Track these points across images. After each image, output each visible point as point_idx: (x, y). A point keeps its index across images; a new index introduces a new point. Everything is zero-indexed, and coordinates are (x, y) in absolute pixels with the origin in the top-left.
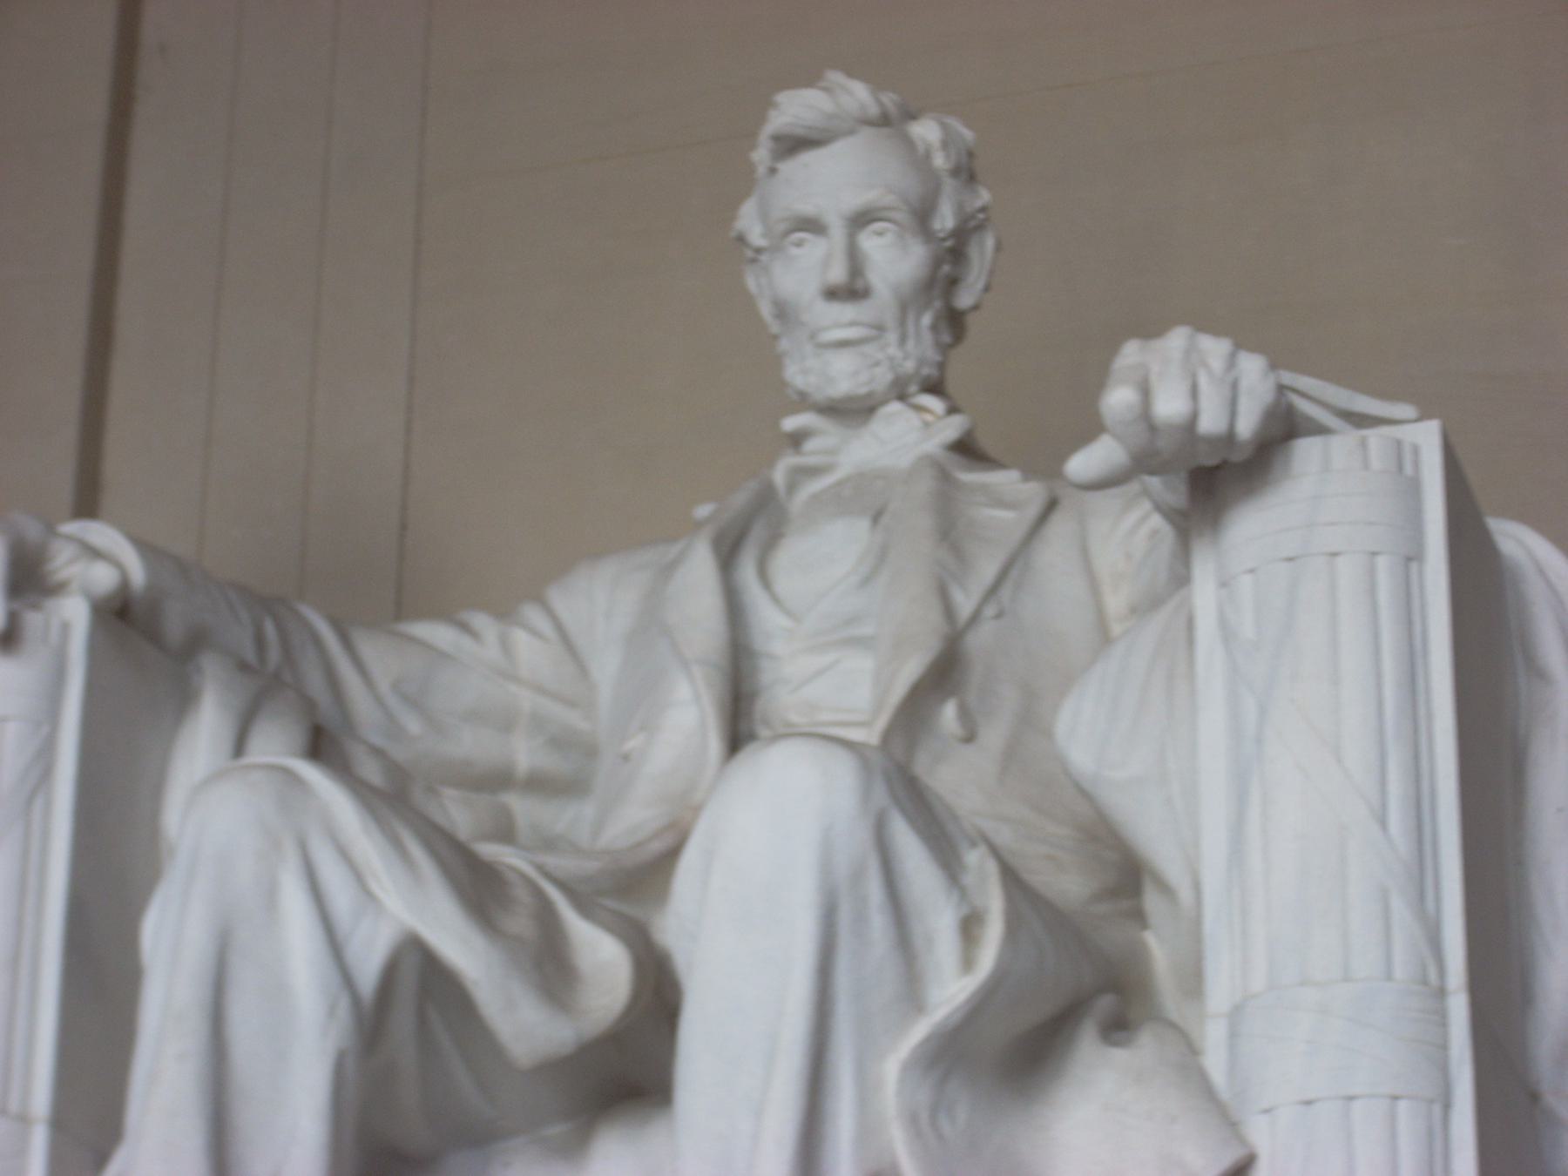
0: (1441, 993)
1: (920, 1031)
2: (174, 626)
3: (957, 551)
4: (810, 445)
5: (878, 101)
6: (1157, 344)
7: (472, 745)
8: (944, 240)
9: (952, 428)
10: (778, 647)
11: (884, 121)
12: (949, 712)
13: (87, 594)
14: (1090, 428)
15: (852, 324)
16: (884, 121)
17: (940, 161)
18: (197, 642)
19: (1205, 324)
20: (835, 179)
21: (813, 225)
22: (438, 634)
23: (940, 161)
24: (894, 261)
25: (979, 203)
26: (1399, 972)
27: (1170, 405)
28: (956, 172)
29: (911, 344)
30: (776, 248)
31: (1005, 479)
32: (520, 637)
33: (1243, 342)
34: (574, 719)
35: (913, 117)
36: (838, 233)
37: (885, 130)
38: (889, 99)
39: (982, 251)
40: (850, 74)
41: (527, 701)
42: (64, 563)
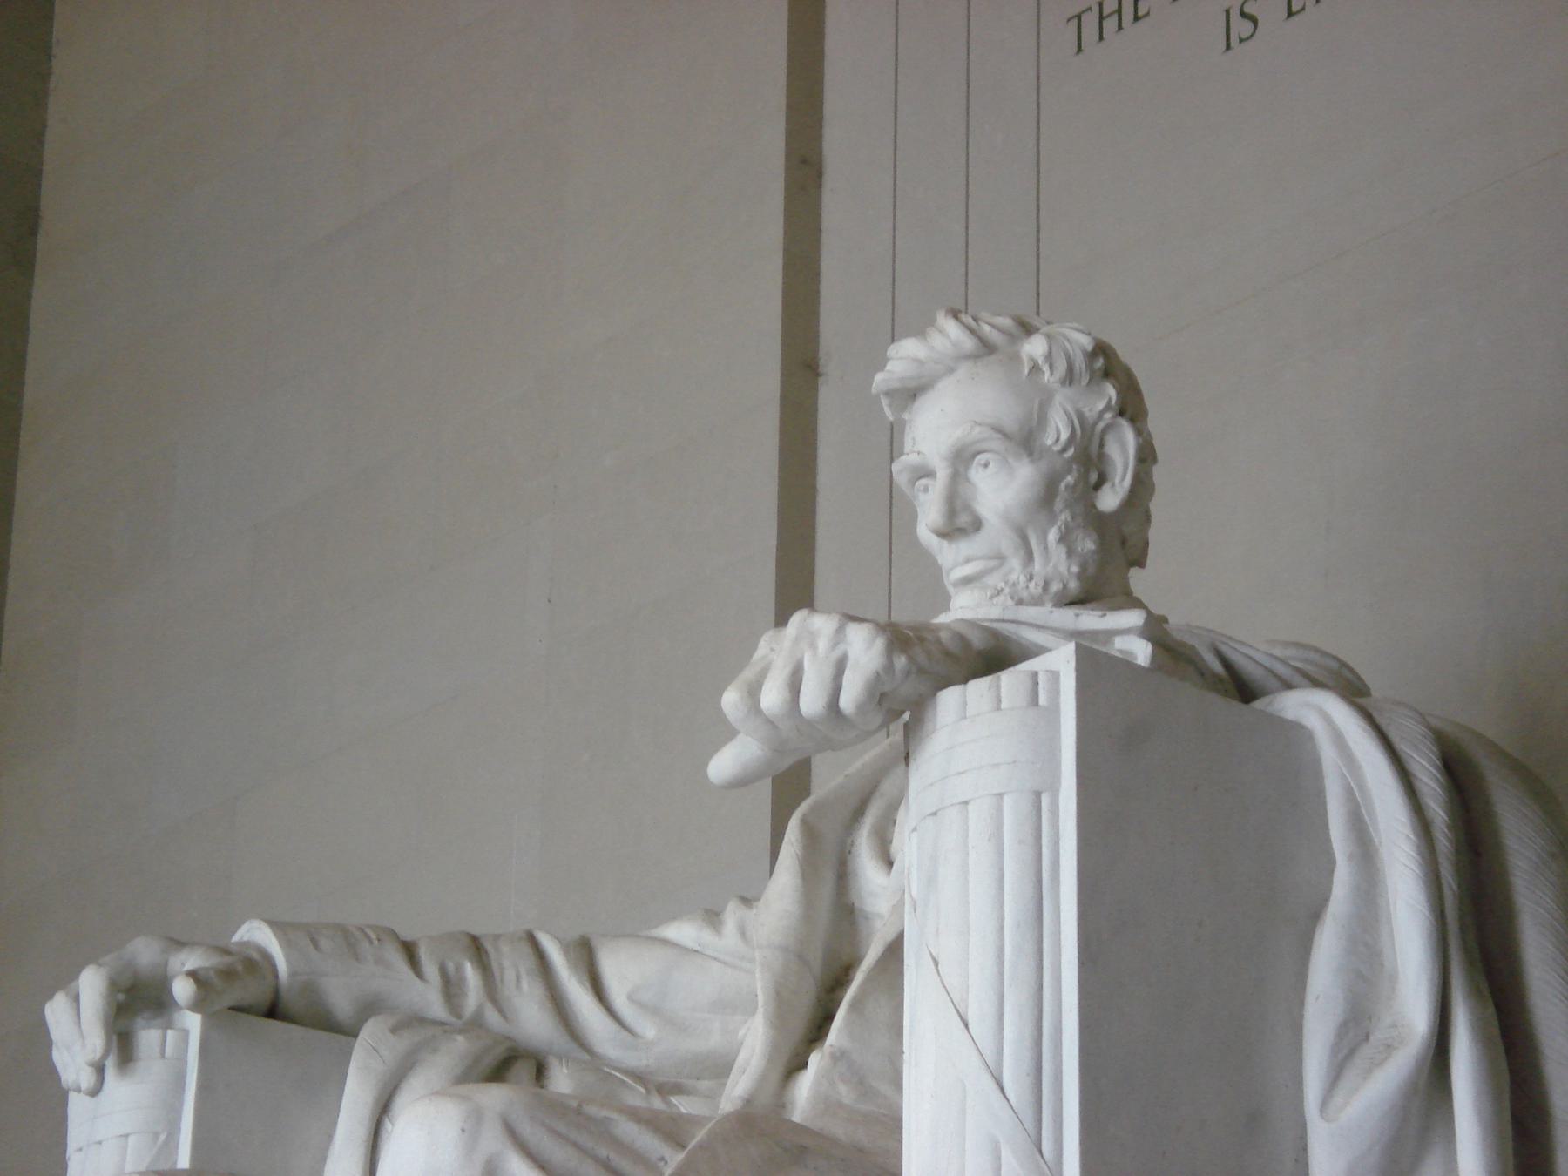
2: (341, 1003)
5: (972, 331)
8: (1064, 450)
11: (987, 348)
14: (728, 733)
15: (968, 560)
16: (987, 348)
18: (370, 1007)
21: (929, 474)
22: (684, 932)
24: (1000, 490)
25: (1101, 405)
27: (772, 697)
28: (1070, 378)
29: (1038, 566)
36: (943, 473)
37: (993, 358)
39: (1122, 449)
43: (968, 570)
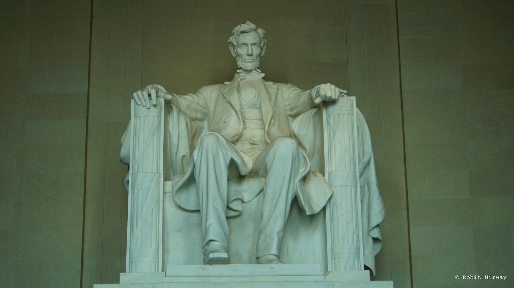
0: (356, 173)
1: (301, 177)
3: (270, 96)
4: (241, 74)
6: (325, 85)
7: (194, 115)
9: (263, 75)
10: (244, 107)
12: (273, 120)
13: (164, 98)
16: (255, 30)
17: (262, 36)
19: (332, 83)
20: (250, 38)
23: (262, 36)
24: (256, 51)
26: (352, 170)
27: (329, 95)
30: (238, 45)
31: (270, 84)
32: (200, 99)
33: (337, 86)
34: (205, 111)
35: (257, 28)
36: (250, 46)
40: (251, 22)
41: (200, 108)
42: (162, 94)
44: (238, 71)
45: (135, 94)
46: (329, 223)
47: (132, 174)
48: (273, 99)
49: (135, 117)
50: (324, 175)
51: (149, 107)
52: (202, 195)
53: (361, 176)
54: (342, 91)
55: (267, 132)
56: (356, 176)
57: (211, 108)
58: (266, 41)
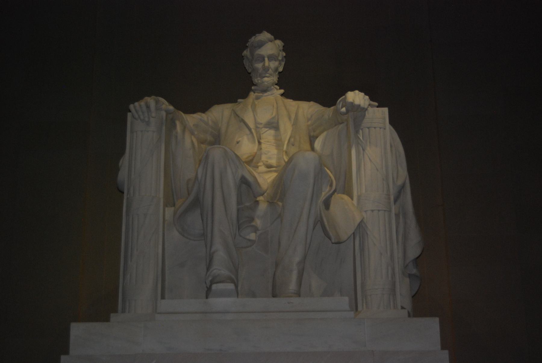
9: (282, 91)
19: (361, 91)
36: (266, 59)
38: (273, 37)
43: (267, 75)
44: (253, 88)
45: (131, 107)
46: (359, 255)
47: (127, 198)
48: (293, 116)
49: (132, 132)
50: (352, 199)
51: (147, 119)
52: (207, 218)
53: (395, 201)
54: (372, 103)
55: (286, 152)
56: (389, 199)
57: (223, 130)
58: (284, 54)
